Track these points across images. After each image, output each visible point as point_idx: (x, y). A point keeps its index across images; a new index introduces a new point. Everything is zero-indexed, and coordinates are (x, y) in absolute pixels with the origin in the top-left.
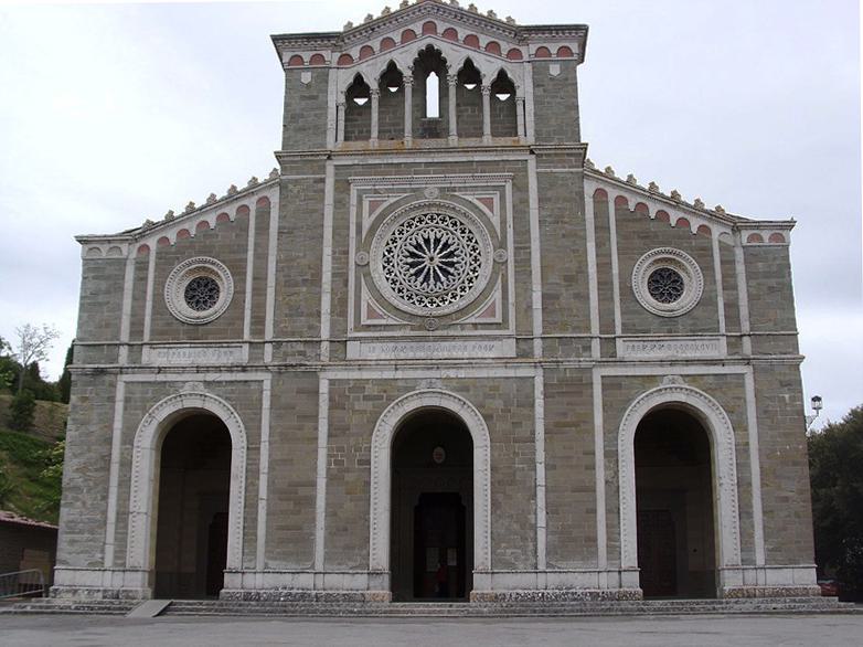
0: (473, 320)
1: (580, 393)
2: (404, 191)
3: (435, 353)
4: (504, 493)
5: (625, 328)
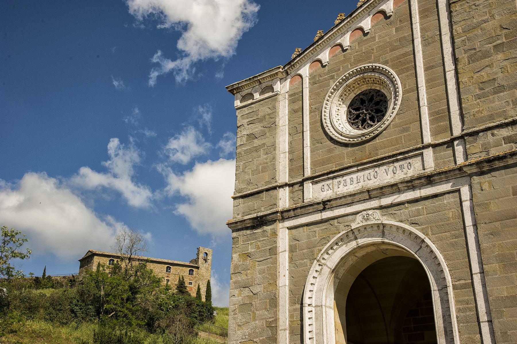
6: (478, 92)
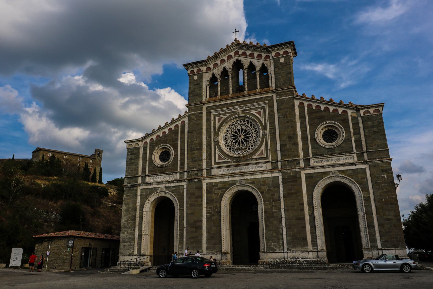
0: (255, 157)
2: (229, 113)
3: (242, 170)
5: (314, 154)
6: (191, 160)
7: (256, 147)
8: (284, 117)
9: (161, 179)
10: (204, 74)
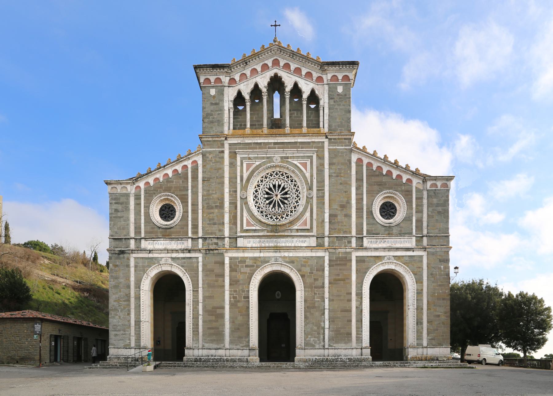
0: (296, 227)
1: (345, 265)
2: (263, 158)
4: (310, 312)
5: (368, 232)
6: (208, 222)
7: (298, 214)
8: (337, 176)
9: (164, 246)
10: (226, 89)
